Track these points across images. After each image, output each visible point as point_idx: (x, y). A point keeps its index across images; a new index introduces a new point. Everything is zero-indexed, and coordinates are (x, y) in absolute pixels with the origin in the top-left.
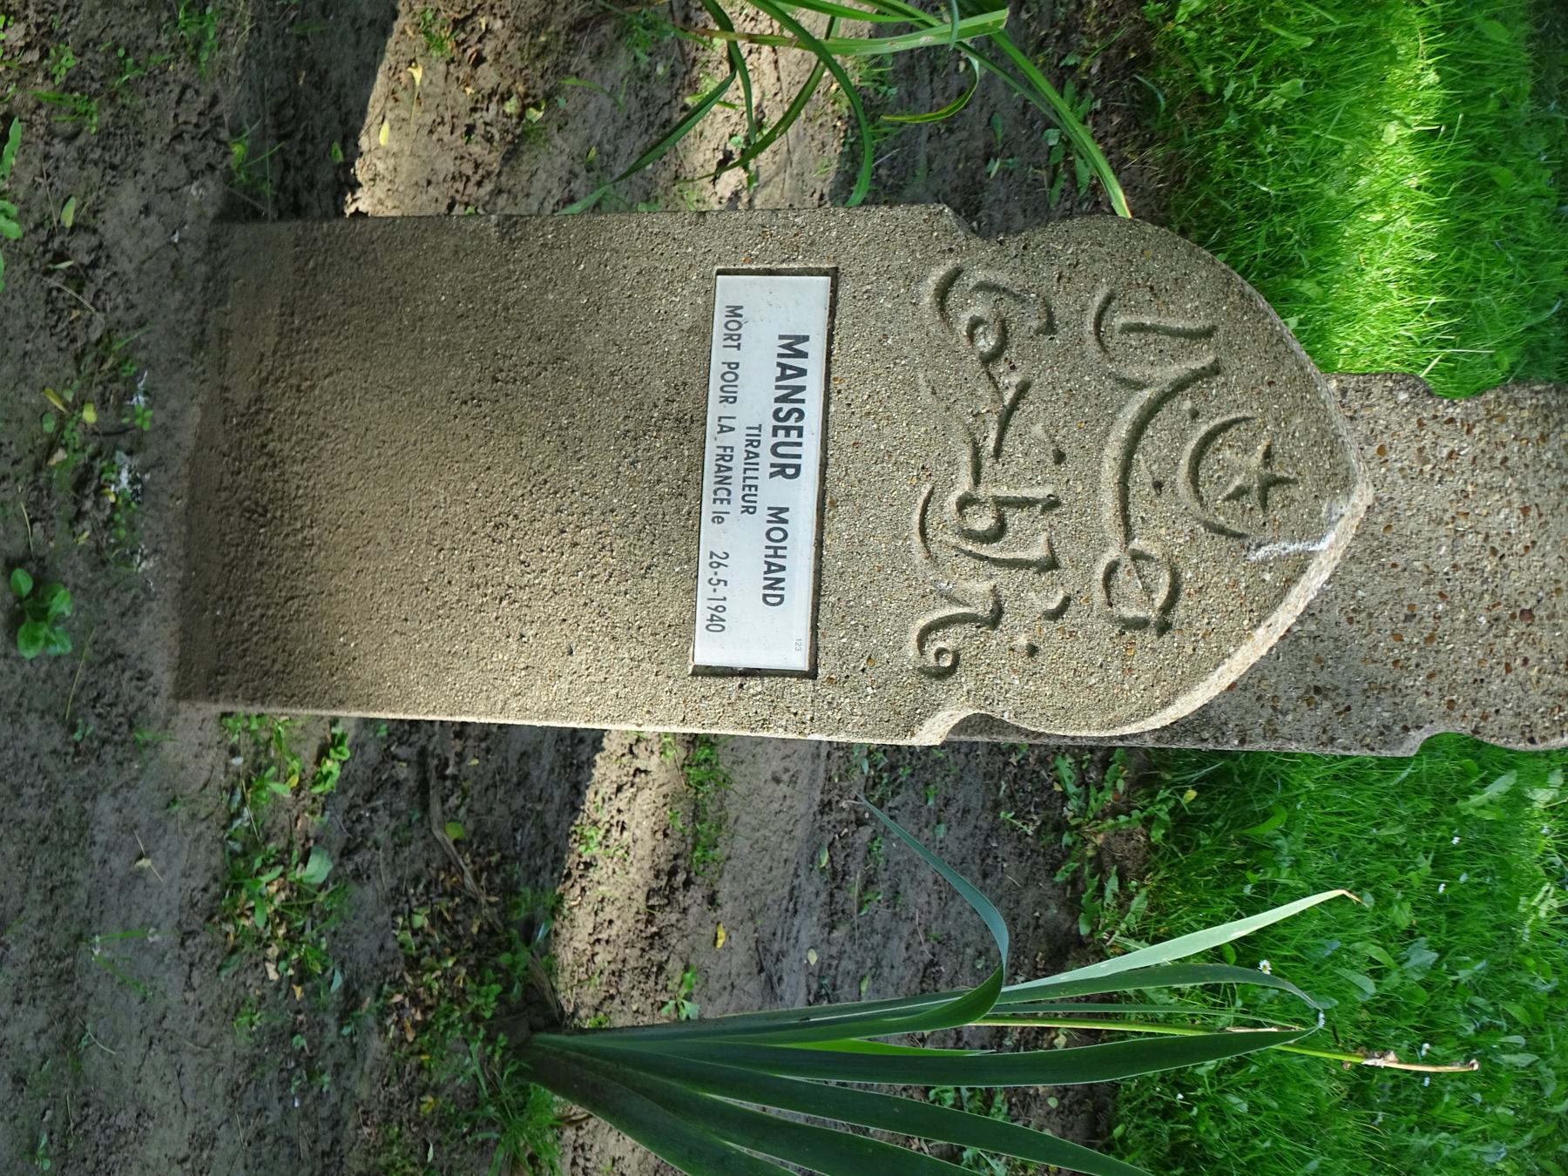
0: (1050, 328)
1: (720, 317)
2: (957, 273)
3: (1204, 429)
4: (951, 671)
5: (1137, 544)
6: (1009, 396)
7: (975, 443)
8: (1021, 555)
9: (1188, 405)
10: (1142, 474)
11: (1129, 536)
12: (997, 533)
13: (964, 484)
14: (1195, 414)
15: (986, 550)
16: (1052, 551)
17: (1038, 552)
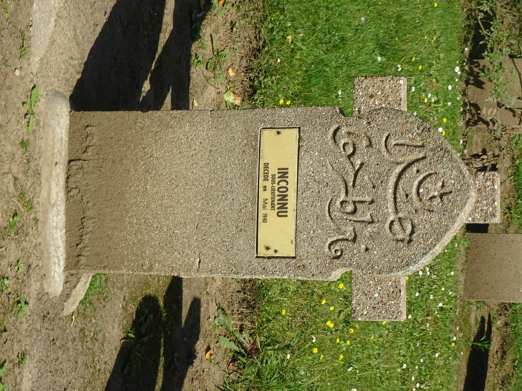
0: (370, 145)
1: (262, 166)
2: (338, 128)
3: (421, 177)
4: (341, 255)
5: (401, 215)
6: (357, 168)
7: (346, 183)
8: (363, 219)
9: (415, 169)
10: (401, 192)
11: (396, 211)
12: (355, 211)
13: (342, 197)
14: (418, 171)
15: (351, 217)
16: (373, 219)
17: (368, 218)
